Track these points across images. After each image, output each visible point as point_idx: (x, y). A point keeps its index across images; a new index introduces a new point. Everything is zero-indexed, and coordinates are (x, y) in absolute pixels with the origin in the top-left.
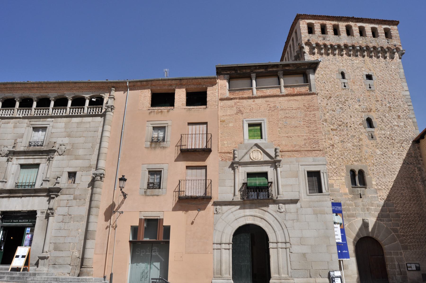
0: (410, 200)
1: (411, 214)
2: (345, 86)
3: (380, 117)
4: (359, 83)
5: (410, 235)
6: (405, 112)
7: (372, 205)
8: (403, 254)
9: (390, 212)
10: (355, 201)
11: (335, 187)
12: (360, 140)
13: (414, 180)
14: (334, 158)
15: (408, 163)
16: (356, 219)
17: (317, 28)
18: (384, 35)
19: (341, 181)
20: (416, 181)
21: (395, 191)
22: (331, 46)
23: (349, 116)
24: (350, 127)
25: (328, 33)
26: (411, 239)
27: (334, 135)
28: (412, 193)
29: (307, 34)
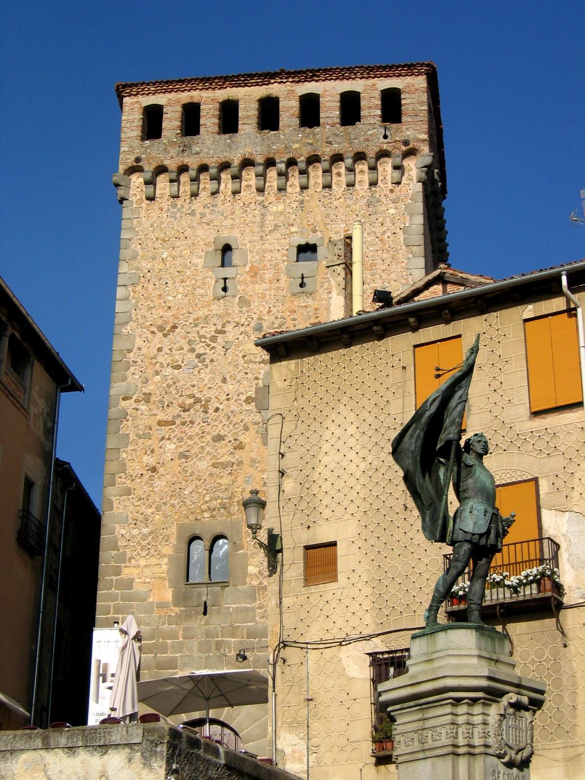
2: (225, 289)
7: (233, 632)
10: (185, 625)
11: (139, 587)
12: (240, 447)
14: (151, 507)
17: (170, 120)
18: (379, 112)
19: (156, 570)
23: (218, 381)
25: (202, 130)
27: (163, 439)
29: (138, 142)
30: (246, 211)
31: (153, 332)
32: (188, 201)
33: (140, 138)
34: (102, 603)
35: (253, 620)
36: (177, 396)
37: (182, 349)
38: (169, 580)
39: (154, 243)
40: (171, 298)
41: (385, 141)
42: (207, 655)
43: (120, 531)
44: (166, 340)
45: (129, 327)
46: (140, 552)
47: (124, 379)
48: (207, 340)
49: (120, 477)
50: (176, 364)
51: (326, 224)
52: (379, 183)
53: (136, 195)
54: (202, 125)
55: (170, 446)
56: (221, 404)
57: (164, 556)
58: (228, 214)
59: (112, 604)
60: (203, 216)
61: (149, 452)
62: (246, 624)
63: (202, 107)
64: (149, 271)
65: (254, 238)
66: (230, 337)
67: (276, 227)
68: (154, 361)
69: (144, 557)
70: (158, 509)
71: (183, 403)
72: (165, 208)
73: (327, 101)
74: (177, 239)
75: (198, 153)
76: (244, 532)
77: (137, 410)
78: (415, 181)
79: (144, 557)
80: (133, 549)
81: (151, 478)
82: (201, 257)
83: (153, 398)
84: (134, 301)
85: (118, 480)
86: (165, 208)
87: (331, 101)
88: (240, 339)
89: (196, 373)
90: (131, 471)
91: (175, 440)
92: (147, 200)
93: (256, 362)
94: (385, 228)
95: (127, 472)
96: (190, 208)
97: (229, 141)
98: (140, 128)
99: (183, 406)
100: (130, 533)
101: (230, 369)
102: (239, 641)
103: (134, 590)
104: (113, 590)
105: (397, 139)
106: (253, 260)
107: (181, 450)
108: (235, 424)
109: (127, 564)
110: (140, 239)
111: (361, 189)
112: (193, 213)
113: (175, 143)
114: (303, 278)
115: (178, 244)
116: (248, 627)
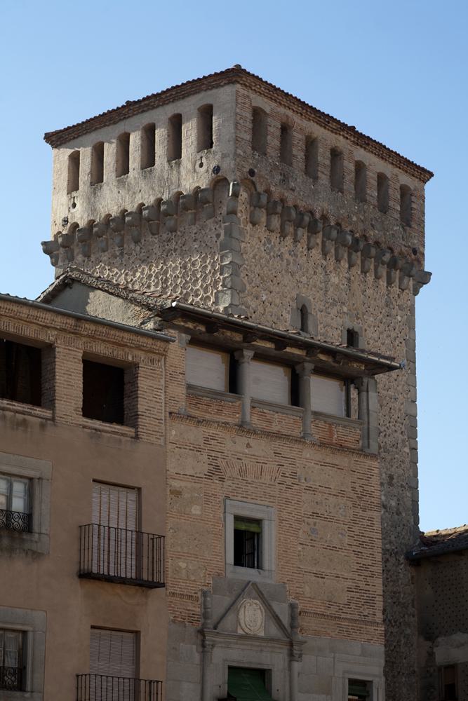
64: (254, 312)
75: (293, 190)
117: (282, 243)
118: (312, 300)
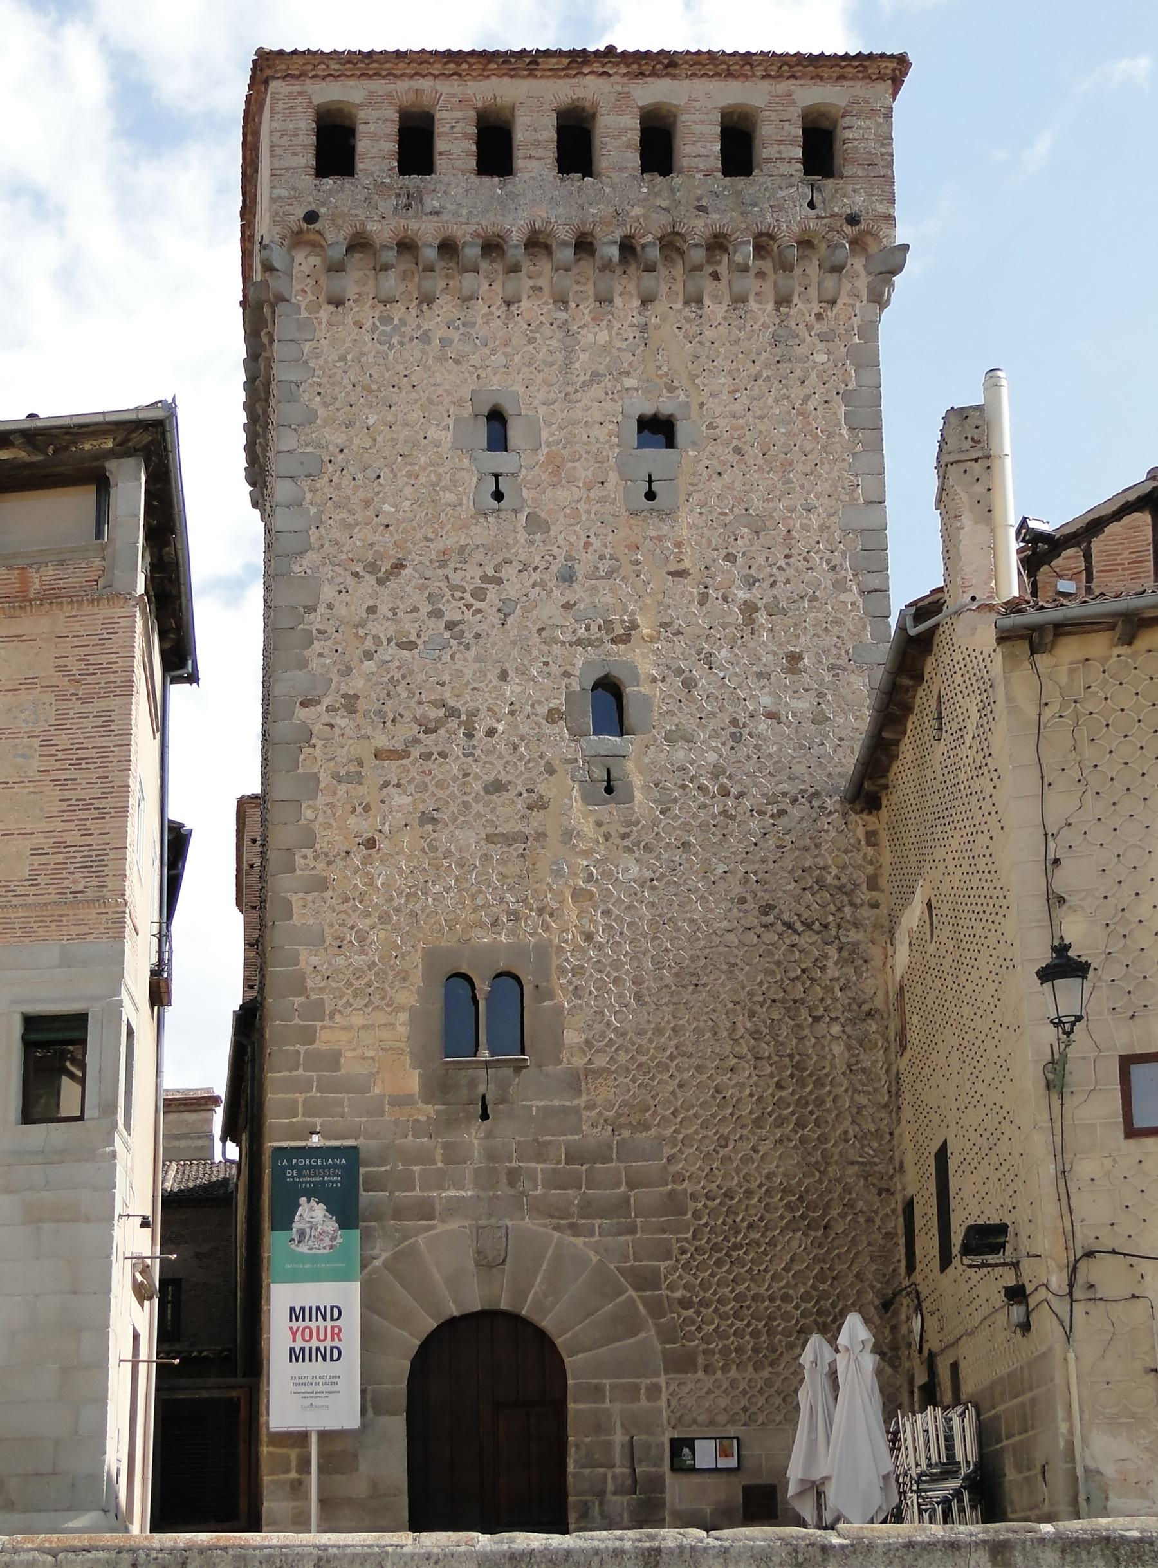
0: (758, 1123)
1: (749, 1193)
2: (498, 496)
3: (679, 672)
4: (584, 472)
5: (722, 1301)
6: (836, 630)
7: (540, 1152)
8: (664, 1396)
9: (631, 1186)
11: (351, 1066)
12: (539, 805)
13: (804, 1013)
14: (368, 914)
15: (789, 926)
16: (441, 1228)
17: (374, 138)
18: (799, 152)
20: (816, 1019)
21: (686, 1076)
22: (448, 248)
24: (491, 732)
25: (440, 163)
26: (724, 1317)
28: (779, 1086)
30: (532, 340)
31: (355, 575)
32: (414, 312)
33: (312, 171)
34: (280, 1096)
35: (577, 1130)
36: (413, 703)
37: (416, 609)
38: (412, 1054)
39: (348, 393)
40: (386, 507)
41: (813, 213)
42: (491, 1193)
43: (308, 959)
44: (384, 592)
45: (305, 562)
46: (351, 1000)
47: (303, 664)
48: (467, 596)
49: (305, 857)
50: (405, 640)
51: (693, 377)
52: (795, 300)
53: (304, 291)
54: (440, 154)
55: (400, 800)
56: (499, 721)
57: (400, 1008)
58: (497, 343)
59: (300, 1098)
60: (445, 343)
61: (359, 810)
62: (564, 1138)
63: (438, 116)
64: (342, 451)
65: (552, 396)
66: (512, 590)
67: (596, 377)
68: (361, 632)
69: (361, 1009)
70: (384, 918)
71: (424, 716)
72: (368, 325)
73: (694, 122)
74: (395, 389)
75: (437, 213)
76: (554, 965)
77: (332, 726)
78: (865, 299)
79: (361, 1009)
80: (337, 994)
81: (367, 860)
82: (447, 428)
83: (362, 705)
84: (313, 510)
85: (299, 861)
86: (368, 325)
87: (702, 122)
88: (532, 596)
89: (446, 657)
90: (324, 845)
91: (411, 789)
92: (329, 303)
93: (563, 643)
94: (808, 391)
95: (317, 846)
96: (419, 327)
97: (499, 191)
98: (312, 151)
99: (424, 722)
100: (330, 964)
101: (515, 653)
102: (554, 1170)
103: (343, 1071)
104: (301, 1071)
105: (836, 209)
106: (551, 439)
107: (421, 807)
108: (529, 761)
109: (327, 1022)
110: (319, 385)
111: (759, 309)
112: (426, 338)
113: (388, 187)
114: (650, 481)
115: (395, 398)
116: (568, 1145)
117: (427, 313)
118: (522, 390)
